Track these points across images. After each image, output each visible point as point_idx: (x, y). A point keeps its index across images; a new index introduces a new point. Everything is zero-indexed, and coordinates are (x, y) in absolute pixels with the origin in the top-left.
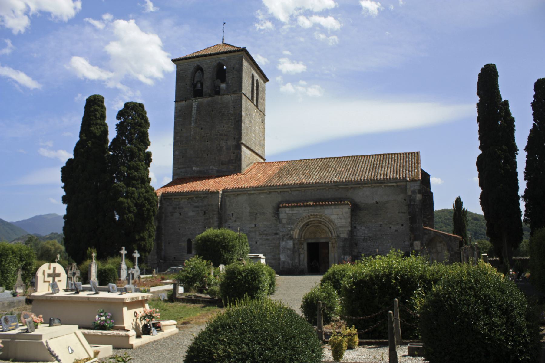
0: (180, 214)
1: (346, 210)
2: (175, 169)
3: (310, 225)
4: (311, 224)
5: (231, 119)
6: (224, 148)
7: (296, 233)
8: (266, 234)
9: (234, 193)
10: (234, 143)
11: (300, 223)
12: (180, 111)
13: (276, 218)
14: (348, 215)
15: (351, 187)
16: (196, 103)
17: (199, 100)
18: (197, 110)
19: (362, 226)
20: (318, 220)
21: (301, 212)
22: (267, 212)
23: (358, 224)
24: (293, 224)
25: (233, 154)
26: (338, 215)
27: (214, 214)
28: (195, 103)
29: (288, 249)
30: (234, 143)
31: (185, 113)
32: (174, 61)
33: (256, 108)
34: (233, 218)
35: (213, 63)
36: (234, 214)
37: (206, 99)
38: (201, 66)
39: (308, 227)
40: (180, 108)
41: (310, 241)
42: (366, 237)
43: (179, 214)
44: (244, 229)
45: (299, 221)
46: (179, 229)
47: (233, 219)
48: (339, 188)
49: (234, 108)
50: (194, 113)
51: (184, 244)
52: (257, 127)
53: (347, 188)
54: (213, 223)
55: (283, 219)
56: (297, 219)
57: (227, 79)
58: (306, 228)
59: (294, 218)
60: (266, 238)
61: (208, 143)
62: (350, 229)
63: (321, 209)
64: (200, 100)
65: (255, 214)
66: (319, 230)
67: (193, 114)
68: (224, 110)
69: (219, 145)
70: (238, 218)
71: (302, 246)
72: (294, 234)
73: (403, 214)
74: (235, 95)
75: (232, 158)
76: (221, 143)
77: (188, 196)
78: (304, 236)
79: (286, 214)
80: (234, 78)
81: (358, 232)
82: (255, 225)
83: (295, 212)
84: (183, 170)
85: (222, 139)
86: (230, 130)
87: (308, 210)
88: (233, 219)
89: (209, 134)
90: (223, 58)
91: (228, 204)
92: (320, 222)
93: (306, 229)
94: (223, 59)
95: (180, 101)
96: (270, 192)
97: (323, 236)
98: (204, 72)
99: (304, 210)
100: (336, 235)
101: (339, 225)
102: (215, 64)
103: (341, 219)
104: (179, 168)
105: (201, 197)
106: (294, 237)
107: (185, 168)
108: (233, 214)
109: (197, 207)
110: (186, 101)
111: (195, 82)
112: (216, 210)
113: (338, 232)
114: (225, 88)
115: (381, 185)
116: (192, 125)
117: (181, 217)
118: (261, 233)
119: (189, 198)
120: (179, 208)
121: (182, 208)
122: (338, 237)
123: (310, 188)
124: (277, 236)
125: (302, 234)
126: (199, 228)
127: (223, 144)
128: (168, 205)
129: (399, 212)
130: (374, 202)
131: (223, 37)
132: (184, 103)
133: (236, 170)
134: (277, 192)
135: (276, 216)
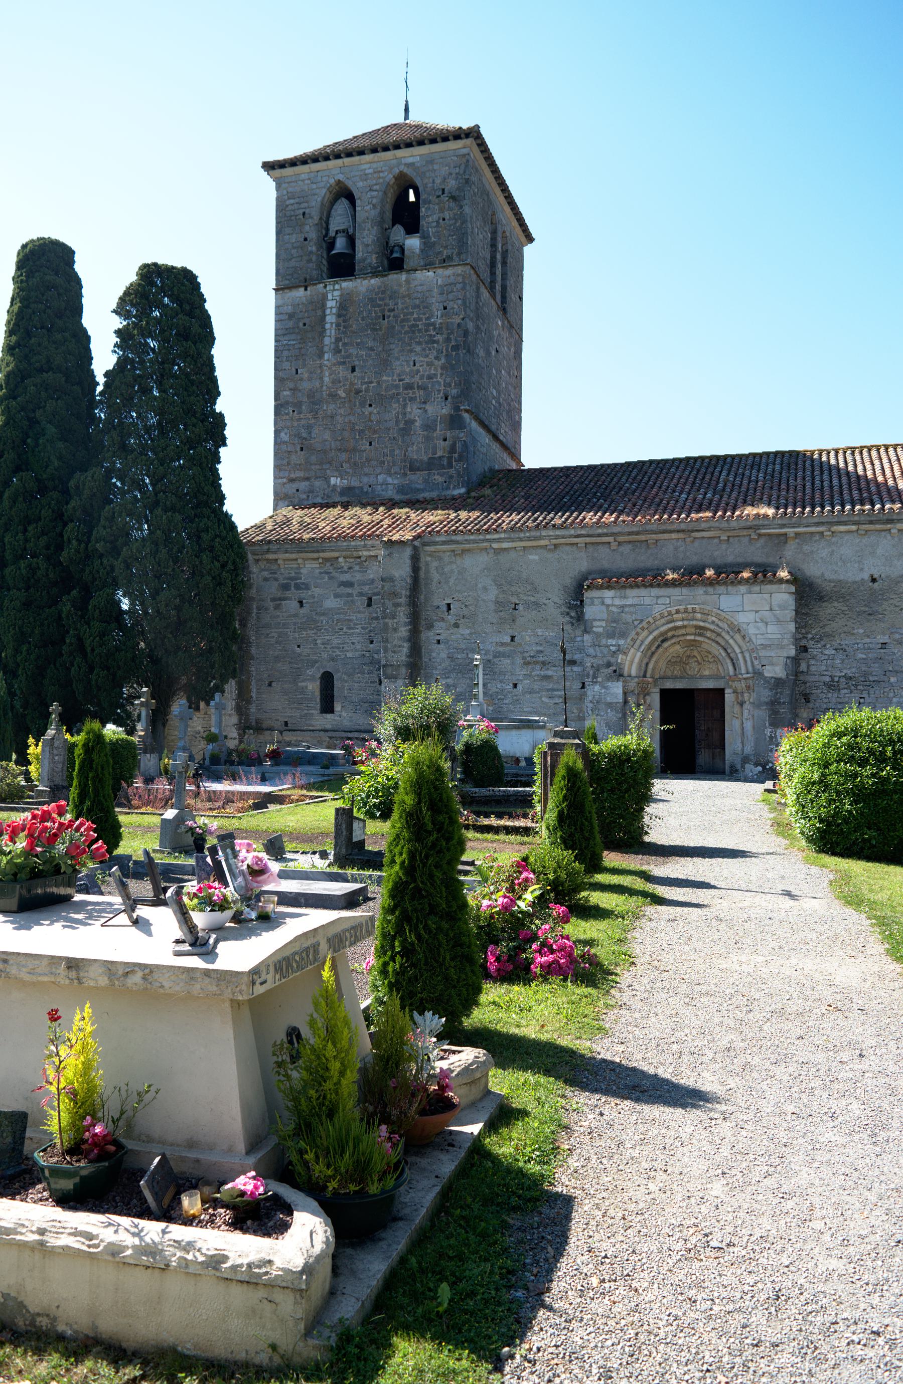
0: (301, 603)
2: (280, 481)
3: (673, 641)
4: (673, 636)
5: (437, 342)
6: (417, 424)
7: (632, 662)
8: (544, 663)
9: (453, 547)
10: (446, 410)
11: (645, 633)
12: (291, 316)
13: (571, 617)
14: (790, 613)
15: (797, 535)
16: (336, 293)
17: (345, 285)
18: (339, 316)
20: (697, 627)
21: (647, 601)
22: (547, 602)
23: (812, 639)
24: (623, 635)
25: (442, 443)
26: (757, 612)
27: (397, 605)
29: (610, 705)
30: (444, 411)
31: (305, 324)
32: (269, 167)
33: (501, 313)
36: (452, 606)
37: (365, 282)
38: (349, 184)
39: (666, 645)
40: (289, 309)
41: (669, 685)
42: (836, 679)
43: (295, 604)
45: (643, 629)
46: (299, 646)
47: (451, 619)
48: (760, 535)
49: (445, 308)
50: (332, 323)
51: (313, 687)
52: (503, 372)
54: (395, 630)
55: (595, 620)
56: (636, 623)
57: (423, 222)
58: (659, 646)
59: (629, 618)
60: (542, 673)
61: (370, 409)
62: (793, 653)
63: (706, 593)
64: (347, 284)
65: (513, 606)
66: (696, 654)
67: (328, 326)
68: (415, 316)
70: (464, 617)
71: (647, 697)
72: (627, 663)
74: (449, 272)
75: (439, 453)
76: (409, 410)
77: (322, 555)
78: (653, 669)
79: (604, 608)
80: (444, 219)
81: (813, 662)
82: (513, 638)
83: (629, 602)
84: (303, 485)
85: (412, 399)
86: (433, 372)
87: (669, 597)
88: (451, 619)
89: (374, 384)
90: (411, 160)
91: (436, 576)
92: (701, 630)
93: (661, 650)
94: (411, 165)
95: (290, 288)
96: (556, 546)
97: (707, 673)
98: (358, 202)
99: (658, 597)
100: (750, 669)
101: (759, 642)
102: (389, 177)
103: (767, 623)
104: (292, 480)
105: (360, 557)
106: (626, 674)
107: (308, 479)
108: (449, 605)
109: (350, 584)
110: (306, 289)
112: (404, 592)
113: (756, 662)
114: (417, 251)
115: (889, 526)
116: (326, 356)
117: (303, 611)
118: (528, 659)
119: (326, 560)
120: (297, 587)
121: (307, 587)
122: (758, 674)
123: (674, 536)
124: (575, 669)
125: (647, 664)
126: (353, 643)
127: (413, 411)
128: (266, 579)
130: (866, 576)
131: (407, 102)
135: (573, 614)
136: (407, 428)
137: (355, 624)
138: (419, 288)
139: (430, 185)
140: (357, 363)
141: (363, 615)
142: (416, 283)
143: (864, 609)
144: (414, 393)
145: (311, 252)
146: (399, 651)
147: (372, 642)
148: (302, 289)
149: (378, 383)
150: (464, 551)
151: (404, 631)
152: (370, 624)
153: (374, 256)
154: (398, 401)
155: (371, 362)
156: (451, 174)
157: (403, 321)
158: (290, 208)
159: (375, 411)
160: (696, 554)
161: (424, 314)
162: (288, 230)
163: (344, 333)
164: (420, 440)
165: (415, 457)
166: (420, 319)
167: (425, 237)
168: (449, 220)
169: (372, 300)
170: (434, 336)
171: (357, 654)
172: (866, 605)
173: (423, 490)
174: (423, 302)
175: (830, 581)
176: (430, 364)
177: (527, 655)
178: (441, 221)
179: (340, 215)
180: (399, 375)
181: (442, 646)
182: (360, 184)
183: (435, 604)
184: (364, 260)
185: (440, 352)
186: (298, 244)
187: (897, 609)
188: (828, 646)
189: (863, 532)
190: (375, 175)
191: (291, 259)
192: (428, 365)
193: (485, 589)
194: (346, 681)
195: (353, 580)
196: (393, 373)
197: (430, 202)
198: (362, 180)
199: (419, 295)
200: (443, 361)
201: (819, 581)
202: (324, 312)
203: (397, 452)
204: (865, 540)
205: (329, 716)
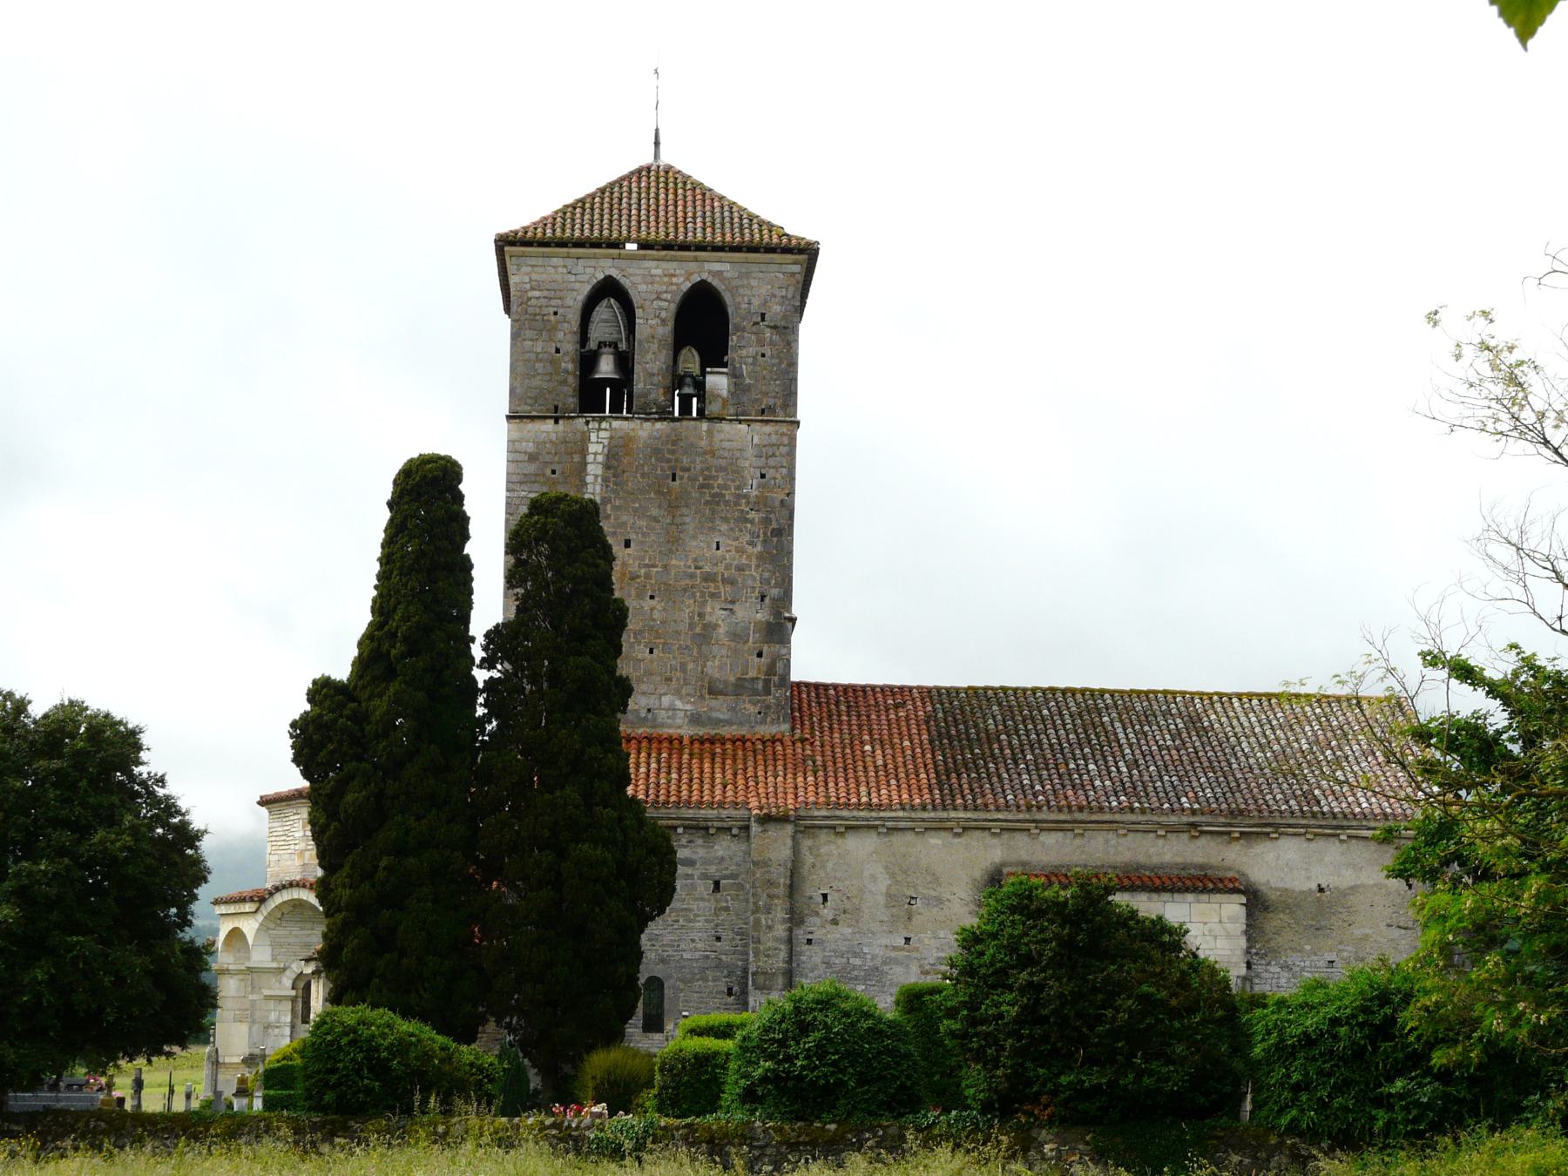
1: (1233, 908)
5: (752, 522)
6: (721, 631)
10: (763, 616)
12: (533, 458)
14: (1241, 926)
18: (607, 467)
19: (1269, 964)
23: (1257, 954)
25: (757, 660)
26: (1205, 923)
28: (599, 436)
31: (554, 472)
34: (826, 911)
35: (674, 280)
37: (647, 425)
38: (626, 282)
40: (530, 447)
44: (866, 950)
48: (1202, 832)
49: (763, 476)
50: (596, 476)
53: (1229, 833)
54: (770, 928)
63: (1150, 899)
67: (589, 479)
68: (720, 481)
69: (701, 615)
70: (845, 912)
73: (1403, 931)
74: (768, 429)
75: (752, 674)
76: (708, 609)
80: (763, 355)
82: (908, 940)
85: (713, 595)
88: (827, 912)
96: (965, 829)
98: (638, 312)
103: (1216, 937)
108: (825, 896)
110: (556, 422)
111: (592, 345)
112: (782, 880)
114: (725, 393)
115: (1339, 832)
118: (927, 967)
126: (693, 941)
127: (715, 612)
129: (1389, 926)
130: (1314, 886)
131: (657, 131)
132: (549, 425)
133: (769, 720)
134: (990, 829)
136: (705, 634)
137: (696, 916)
138: (726, 444)
139: (744, 306)
140: (632, 536)
141: (707, 904)
142: (722, 436)
143: (1311, 922)
144: (717, 587)
145: (566, 371)
146: (775, 956)
147: (719, 939)
148: (552, 421)
149: (665, 567)
150: (848, 828)
151: (780, 930)
152: (718, 916)
153: (661, 391)
154: (694, 595)
155: (653, 537)
156: (775, 296)
157: (702, 486)
158: (533, 302)
159: (659, 607)
160: (1129, 849)
161: (734, 481)
162: (529, 334)
163: (614, 491)
164: (724, 652)
165: (717, 675)
166: (727, 487)
167: (735, 376)
168: (772, 357)
169: (656, 451)
170: (747, 513)
171: (697, 955)
172: (1313, 919)
173: (729, 723)
174: (732, 464)
175: (1276, 889)
176: (740, 551)
177: (926, 962)
178: (759, 357)
179: (606, 321)
180: (695, 560)
181: (814, 947)
182: (643, 287)
183: (807, 894)
184: (645, 395)
185: (755, 535)
186: (546, 356)
187: (1345, 925)
188: (1273, 963)
189: (1311, 837)
190: (666, 279)
191: (534, 376)
192: (737, 551)
193: (872, 876)
194: (682, 990)
195: (694, 857)
196: (687, 556)
197: (744, 330)
198: (647, 284)
199: (726, 454)
200: (759, 548)
201: (1263, 888)
202: (584, 457)
203: (690, 666)
204: (1313, 845)
205: (657, 1036)
